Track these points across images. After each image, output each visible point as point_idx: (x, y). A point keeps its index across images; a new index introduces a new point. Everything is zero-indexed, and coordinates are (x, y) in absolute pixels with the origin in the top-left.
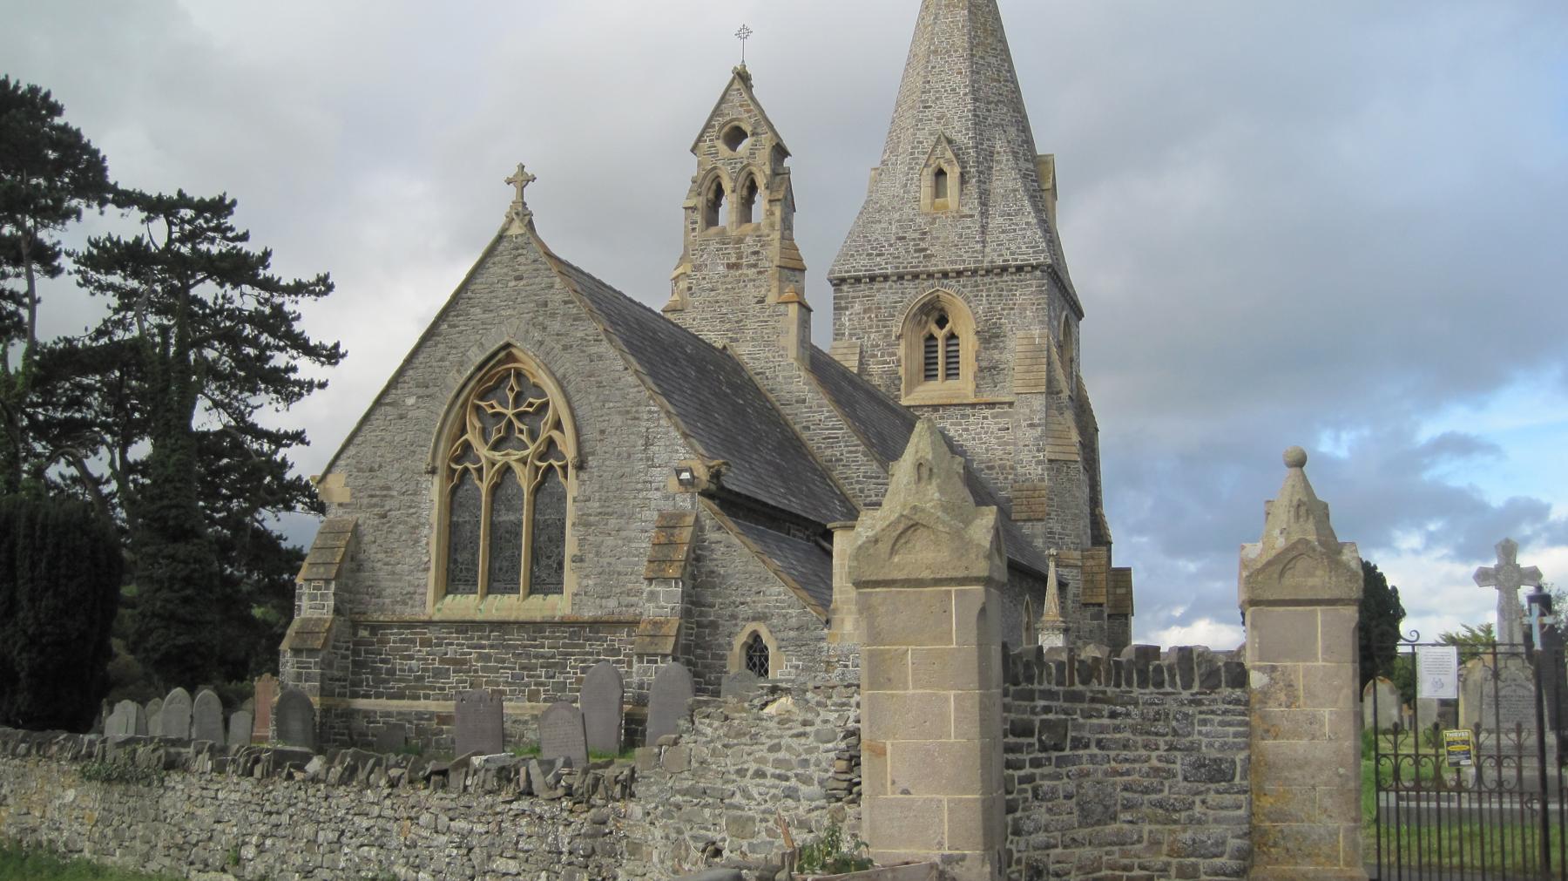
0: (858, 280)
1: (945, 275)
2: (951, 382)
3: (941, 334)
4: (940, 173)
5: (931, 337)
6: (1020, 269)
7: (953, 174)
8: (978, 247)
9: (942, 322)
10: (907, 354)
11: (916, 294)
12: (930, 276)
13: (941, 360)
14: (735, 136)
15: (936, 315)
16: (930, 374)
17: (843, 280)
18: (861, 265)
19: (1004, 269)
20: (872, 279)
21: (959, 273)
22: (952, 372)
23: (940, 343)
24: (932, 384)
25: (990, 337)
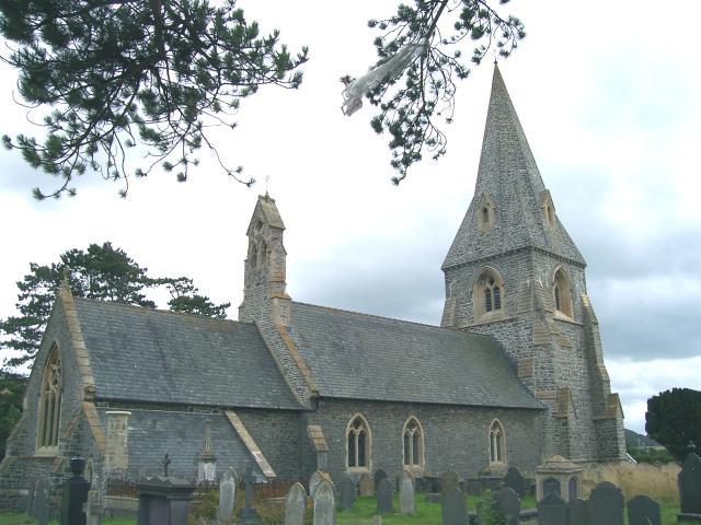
0: (453, 268)
1: (488, 259)
2: (498, 312)
3: (491, 288)
4: (485, 211)
5: (488, 290)
6: (518, 250)
7: (490, 211)
8: (500, 243)
9: (492, 282)
10: (478, 299)
11: (477, 271)
12: (482, 261)
13: (493, 301)
14: (260, 224)
15: (488, 280)
16: (489, 309)
17: (448, 269)
18: (455, 261)
19: (512, 252)
20: (459, 266)
21: (494, 257)
22: (498, 307)
23: (492, 292)
24: (490, 313)
25: (511, 288)
